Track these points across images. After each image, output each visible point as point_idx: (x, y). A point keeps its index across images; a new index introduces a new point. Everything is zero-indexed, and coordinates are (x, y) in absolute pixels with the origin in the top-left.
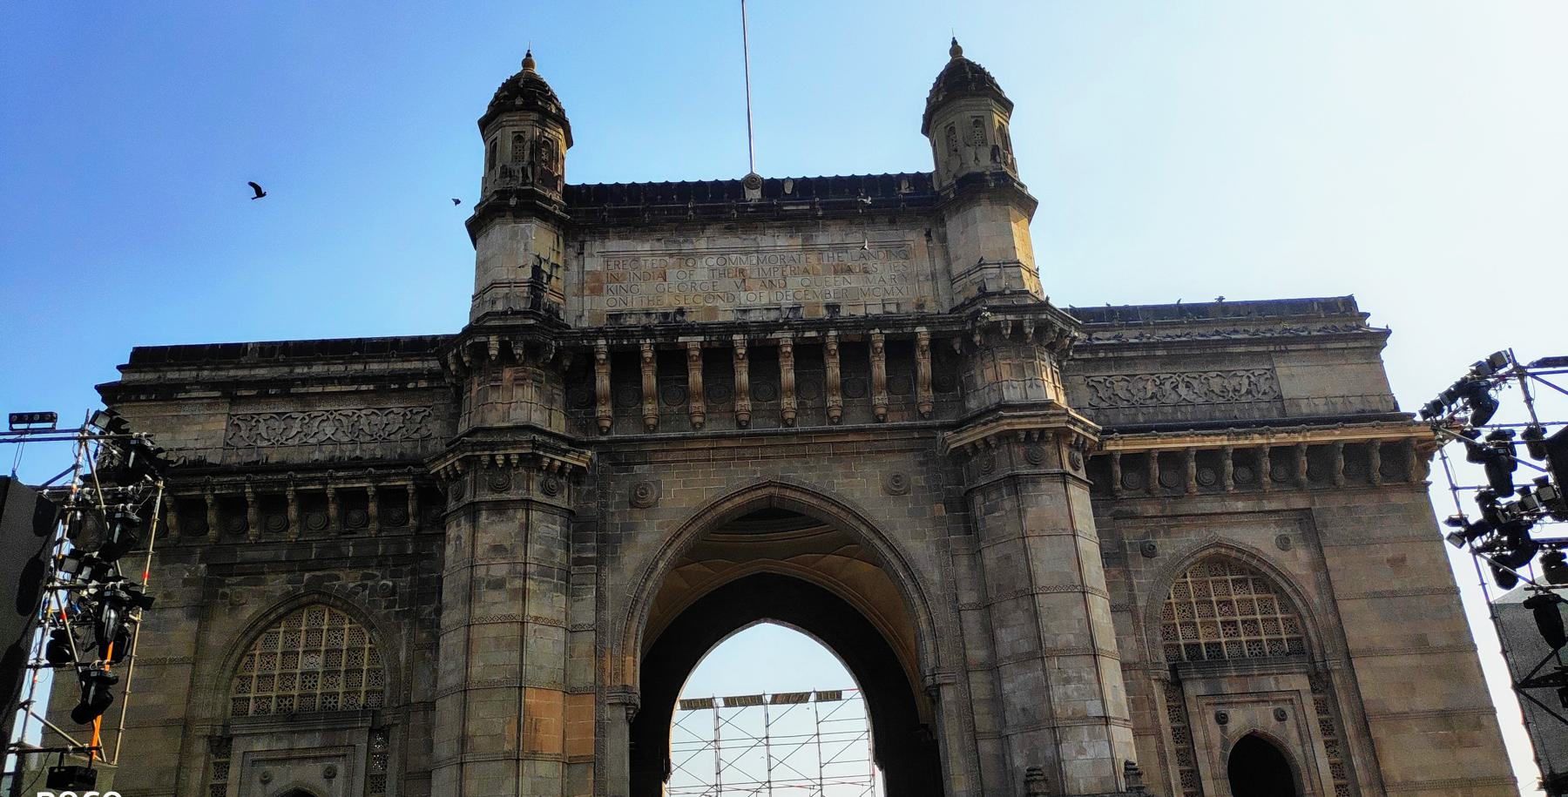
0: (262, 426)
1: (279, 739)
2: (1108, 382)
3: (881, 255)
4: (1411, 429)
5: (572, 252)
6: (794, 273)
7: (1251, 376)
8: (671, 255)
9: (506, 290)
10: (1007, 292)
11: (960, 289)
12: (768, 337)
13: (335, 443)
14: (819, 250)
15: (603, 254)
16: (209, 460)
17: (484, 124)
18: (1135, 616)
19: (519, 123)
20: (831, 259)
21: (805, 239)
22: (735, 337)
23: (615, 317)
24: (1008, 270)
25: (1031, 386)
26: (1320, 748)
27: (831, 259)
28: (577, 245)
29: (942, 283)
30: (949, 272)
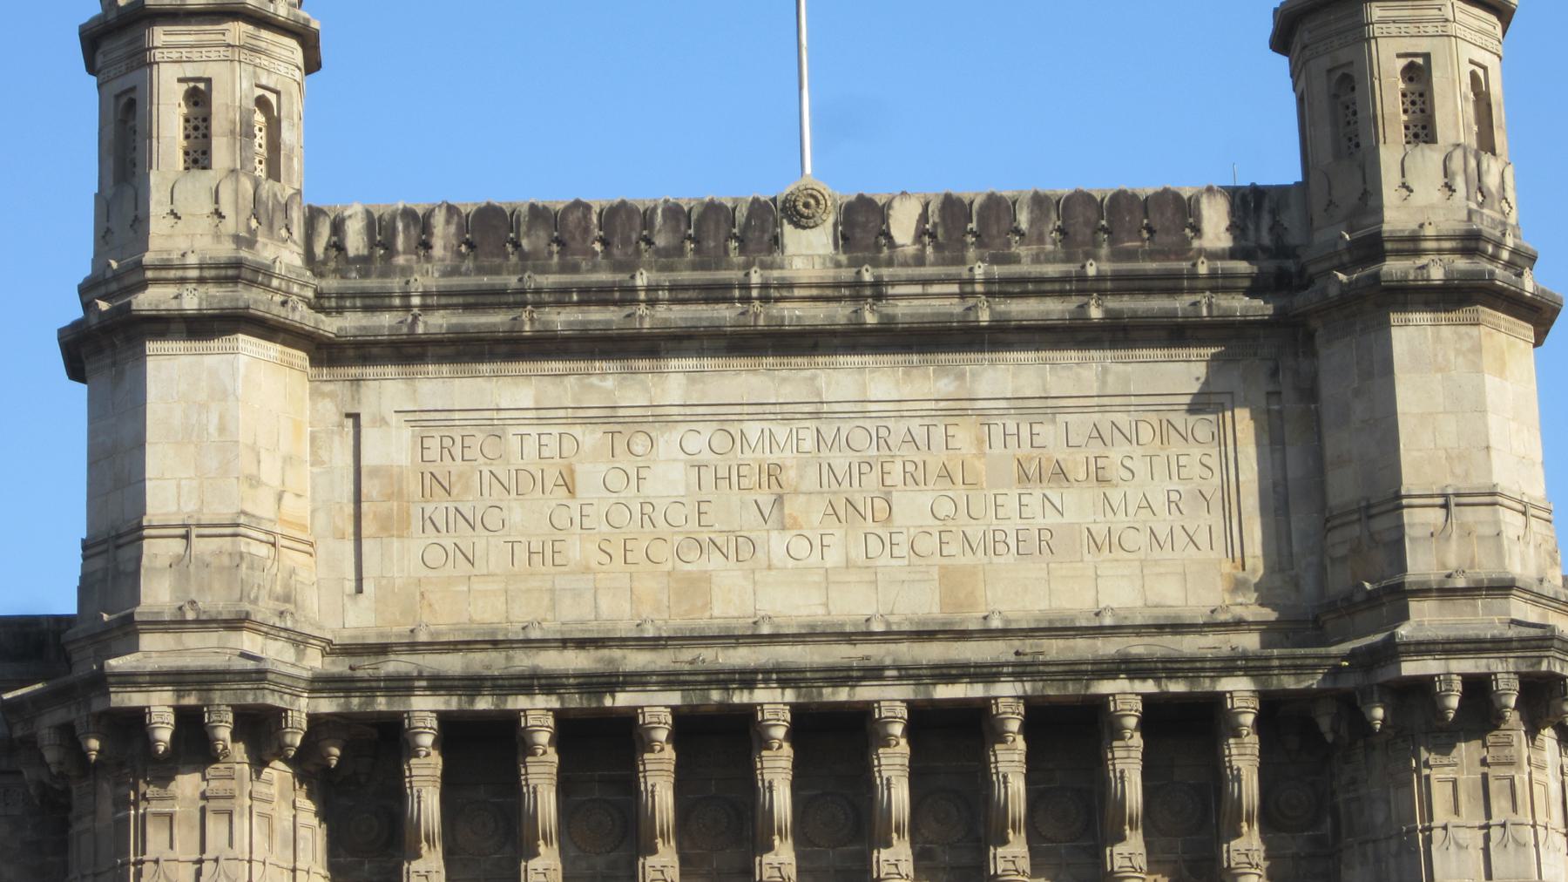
3: (1146, 433)
5: (329, 410)
6: (911, 479)
8: (588, 422)
9: (177, 546)
10: (1460, 582)
11: (1341, 551)
12: (843, 695)
14: (981, 413)
15: (420, 419)
17: (94, 39)
19: (195, 55)
20: (1012, 441)
22: (760, 695)
24: (1469, 515)
27: (1012, 441)
29: (1301, 521)
30: (1322, 488)
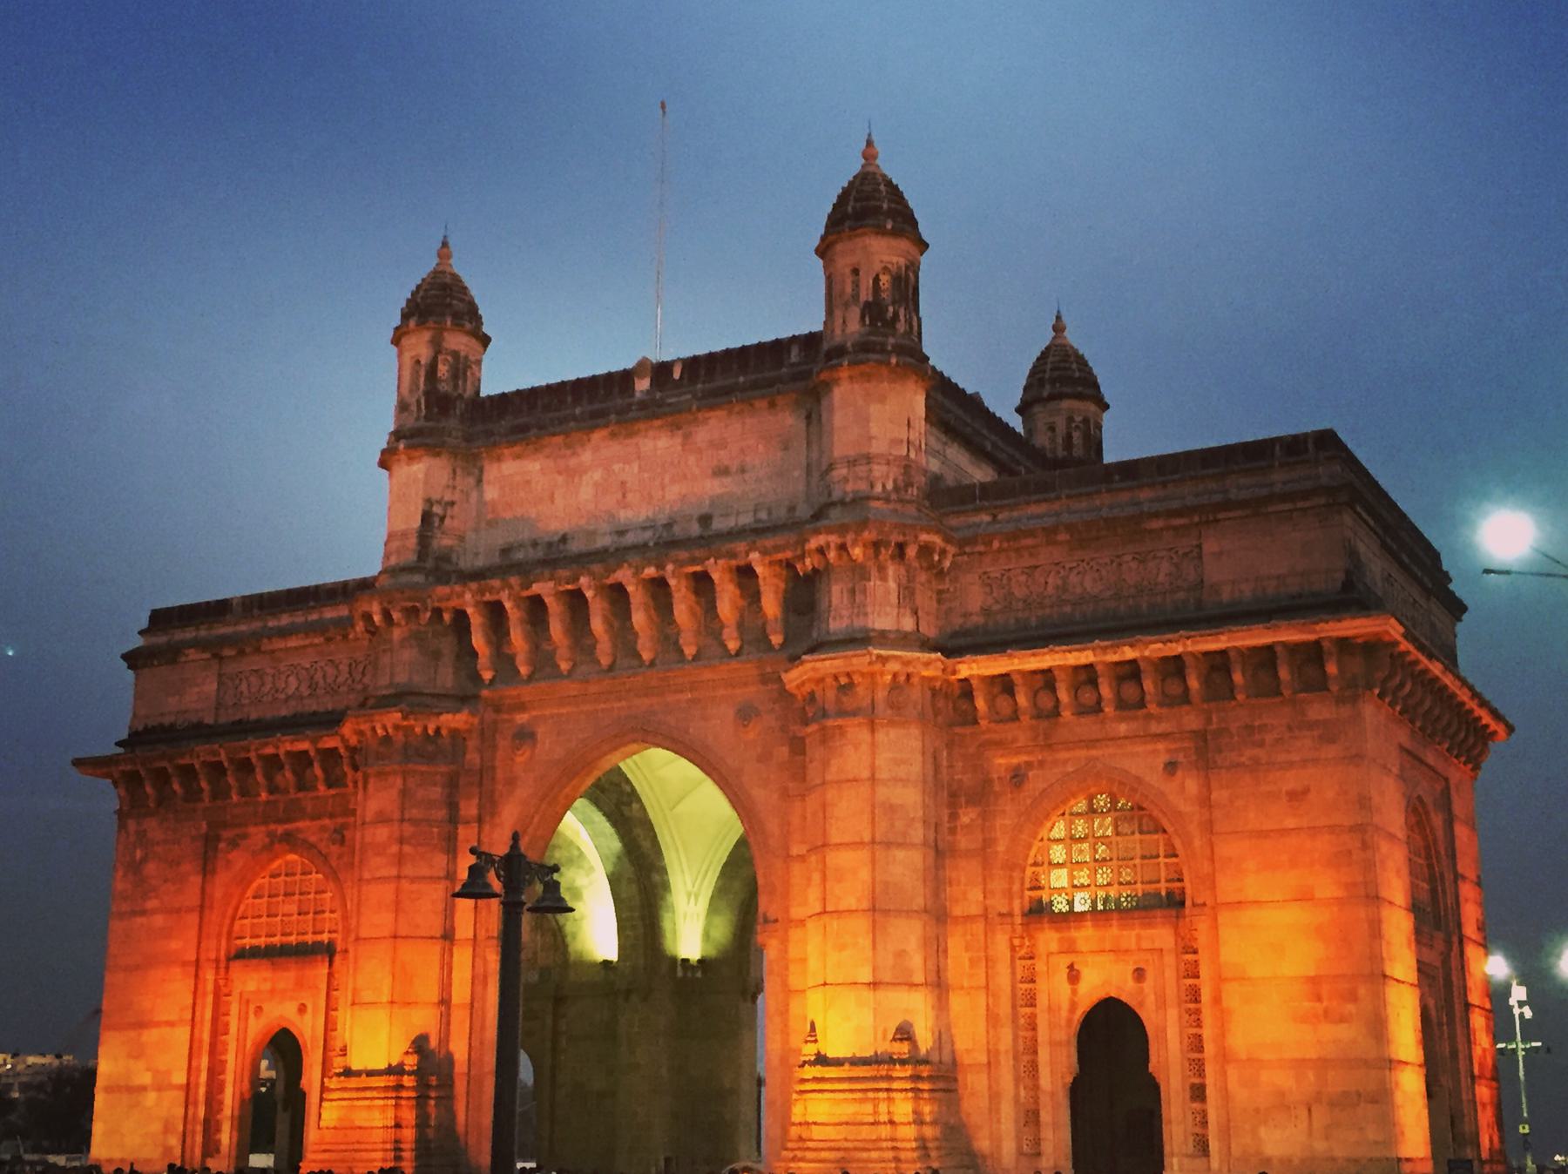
0: (244, 682)
1: (265, 980)
2: (1005, 581)
4: (1318, 628)
6: (673, 481)
7: (1174, 556)
8: (560, 473)
13: (302, 698)
14: (700, 451)
16: (206, 721)
18: (986, 864)
21: (687, 437)
23: (506, 551)
25: (858, 615)
26: (1172, 1014)
28: (476, 471)
